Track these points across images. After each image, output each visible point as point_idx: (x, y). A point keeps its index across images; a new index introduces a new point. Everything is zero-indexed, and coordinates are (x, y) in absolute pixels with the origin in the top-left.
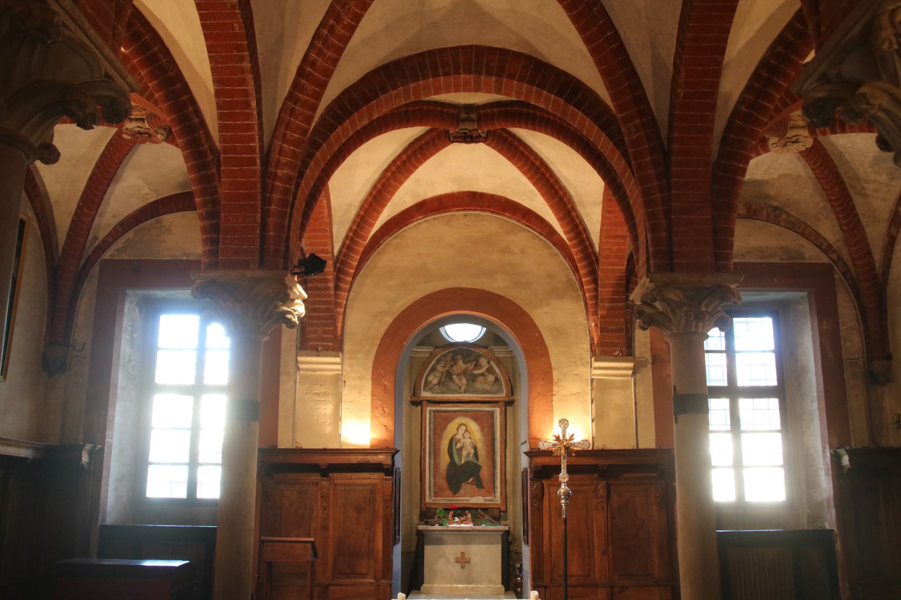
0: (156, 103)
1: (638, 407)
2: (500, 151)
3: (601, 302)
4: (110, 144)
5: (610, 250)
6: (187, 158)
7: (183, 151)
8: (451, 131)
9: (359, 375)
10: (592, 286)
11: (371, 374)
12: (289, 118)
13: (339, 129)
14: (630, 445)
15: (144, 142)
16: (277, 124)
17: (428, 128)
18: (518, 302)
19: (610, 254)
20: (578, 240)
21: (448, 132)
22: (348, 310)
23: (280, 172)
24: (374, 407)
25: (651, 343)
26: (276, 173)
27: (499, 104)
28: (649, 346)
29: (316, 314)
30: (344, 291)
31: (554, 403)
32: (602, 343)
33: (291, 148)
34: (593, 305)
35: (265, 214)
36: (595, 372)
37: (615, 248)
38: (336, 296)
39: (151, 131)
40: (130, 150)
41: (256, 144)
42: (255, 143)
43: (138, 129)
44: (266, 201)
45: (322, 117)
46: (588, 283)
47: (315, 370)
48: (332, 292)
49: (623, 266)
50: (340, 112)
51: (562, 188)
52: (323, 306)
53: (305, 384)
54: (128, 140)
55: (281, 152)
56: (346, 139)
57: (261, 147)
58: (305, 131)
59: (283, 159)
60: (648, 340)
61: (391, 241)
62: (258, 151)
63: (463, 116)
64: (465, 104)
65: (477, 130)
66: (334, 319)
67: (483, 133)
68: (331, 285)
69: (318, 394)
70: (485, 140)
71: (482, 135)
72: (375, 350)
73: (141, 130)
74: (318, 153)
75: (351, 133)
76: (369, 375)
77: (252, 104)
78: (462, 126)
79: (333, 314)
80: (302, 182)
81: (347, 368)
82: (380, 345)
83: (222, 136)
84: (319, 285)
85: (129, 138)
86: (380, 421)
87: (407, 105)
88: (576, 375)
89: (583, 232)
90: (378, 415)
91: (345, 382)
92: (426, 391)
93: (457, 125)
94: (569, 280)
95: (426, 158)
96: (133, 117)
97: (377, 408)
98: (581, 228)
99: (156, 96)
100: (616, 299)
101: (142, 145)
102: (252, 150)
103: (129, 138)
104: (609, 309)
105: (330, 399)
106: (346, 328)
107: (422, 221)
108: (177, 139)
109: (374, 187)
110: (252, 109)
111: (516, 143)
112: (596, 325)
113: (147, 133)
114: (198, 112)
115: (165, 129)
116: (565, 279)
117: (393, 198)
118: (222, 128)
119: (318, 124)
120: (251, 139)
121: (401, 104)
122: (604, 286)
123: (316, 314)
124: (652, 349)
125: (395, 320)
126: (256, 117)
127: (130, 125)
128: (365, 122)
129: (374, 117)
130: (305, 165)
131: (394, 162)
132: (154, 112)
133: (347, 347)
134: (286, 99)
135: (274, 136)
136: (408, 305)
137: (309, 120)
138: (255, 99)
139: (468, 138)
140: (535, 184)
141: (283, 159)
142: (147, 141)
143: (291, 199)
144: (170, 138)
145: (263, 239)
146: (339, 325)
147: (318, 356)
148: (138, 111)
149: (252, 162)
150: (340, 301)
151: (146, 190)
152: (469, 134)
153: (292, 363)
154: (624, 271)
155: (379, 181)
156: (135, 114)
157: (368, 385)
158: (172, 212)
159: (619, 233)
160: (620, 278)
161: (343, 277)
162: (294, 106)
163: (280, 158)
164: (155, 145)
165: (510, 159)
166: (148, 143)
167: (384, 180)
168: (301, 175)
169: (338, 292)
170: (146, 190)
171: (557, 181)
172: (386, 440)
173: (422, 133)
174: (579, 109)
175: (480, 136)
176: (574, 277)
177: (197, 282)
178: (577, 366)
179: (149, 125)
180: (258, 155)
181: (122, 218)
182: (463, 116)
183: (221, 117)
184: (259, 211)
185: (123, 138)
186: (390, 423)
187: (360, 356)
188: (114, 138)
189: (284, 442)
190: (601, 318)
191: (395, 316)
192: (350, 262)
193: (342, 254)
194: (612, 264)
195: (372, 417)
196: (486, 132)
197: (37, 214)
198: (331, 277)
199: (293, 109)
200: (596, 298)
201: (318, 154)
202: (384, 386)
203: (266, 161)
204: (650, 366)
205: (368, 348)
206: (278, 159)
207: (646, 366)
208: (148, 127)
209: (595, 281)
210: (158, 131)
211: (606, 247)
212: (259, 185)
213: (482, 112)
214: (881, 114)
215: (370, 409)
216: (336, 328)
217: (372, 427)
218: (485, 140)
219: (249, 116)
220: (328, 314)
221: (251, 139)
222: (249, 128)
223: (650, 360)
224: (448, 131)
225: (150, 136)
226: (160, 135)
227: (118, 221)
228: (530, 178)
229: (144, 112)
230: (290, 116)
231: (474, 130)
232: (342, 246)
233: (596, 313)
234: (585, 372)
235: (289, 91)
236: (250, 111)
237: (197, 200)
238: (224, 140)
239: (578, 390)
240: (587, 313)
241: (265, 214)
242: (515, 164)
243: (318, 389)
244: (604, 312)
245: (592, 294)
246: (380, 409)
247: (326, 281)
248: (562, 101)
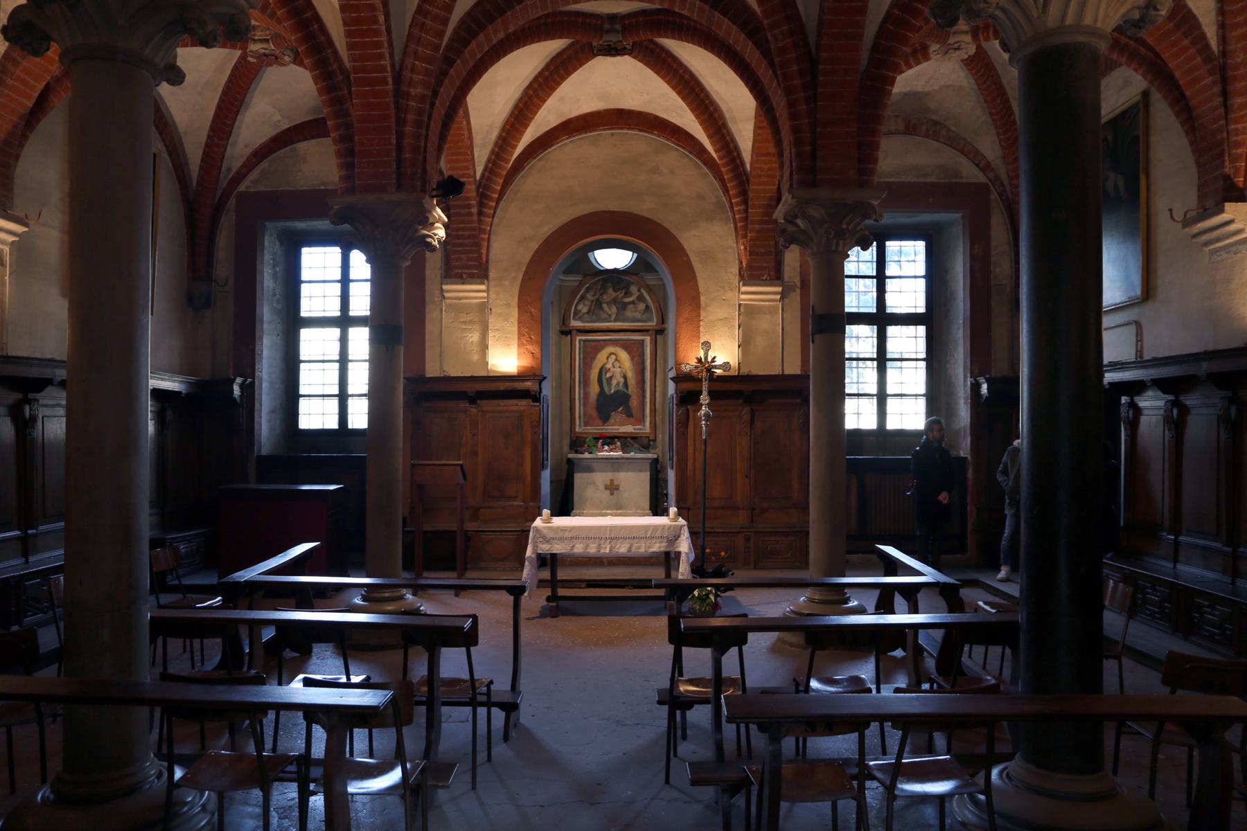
0: (279, 21)
1: (785, 332)
2: (647, 64)
3: (751, 224)
4: (235, 68)
6: (315, 79)
7: (311, 72)
8: (595, 44)
9: (505, 302)
10: (742, 207)
11: (517, 301)
12: (419, 33)
13: (473, 44)
14: (776, 370)
15: (270, 65)
16: (407, 41)
17: (571, 41)
18: (666, 225)
19: (762, 173)
21: (591, 45)
22: (492, 236)
23: (413, 92)
24: (520, 335)
25: (801, 267)
26: (408, 93)
27: (644, 12)
28: (799, 271)
29: (460, 241)
31: (701, 329)
32: (750, 267)
33: (424, 65)
34: (743, 228)
35: (400, 136)
36: (743, 297)
37: (766, 167)
38: (480, 222)
39: (277, 52)
40: (257, 74)
41: (387, 63)
42: (386, 61)
43: (263, 51)
44: (401, 122)
45: (455, 31)
46: (738, 204)
47: (460, 299)
48: (475, 218)
49: (774, 185)
50: (473, 26)
51: (713, 103)
52: (467, 233)
53: (451, 312)
54: (254, 63)
55: (413, 69)
56: (481, 55)
57: (393, 65)
58: (438, 47)
59: (416, 77)
60: (798, 264)
62: (389, 69)
63: (607, 26)
64: (608, 14)
65: (621, 41)
66: (479, 246)
67: (628, 44)
68: (475, 210)
69: (464, 322)
70: (630, 53)
71: (627, 46)
72: (520, 277)
73: (267, 52)
74: (452, 70)
75: (486, 48)
76: (515, 302)
77: (380, 19)
78: (605, 38)
79: (477, 241)
80: (437, 102)
81: (493, 295)
82: (526, 272)
83: (351, 54)
84: (463, 211)
85: (255, 60)
86: (527, 349)
87: (546, 16)
88: (724, 300)
89: (733, 149)
90: (525, 342)
91: (491, 309)
92: (576, 320)
93: (601, 37)
95: (569, 73)
96: (256, 38)
97: (524, 335)
98: (732, 145)
99: (279, 13)
101: (269, 68)
102: (383, 69)
103: (255, 60)
105: (476, 327)
106: (491, 254)
107: (568, 141)
108: (304, 59)
109: (516, 106)
110: (381, 25)
111: (664, 55)
112: (745, 248)
113: (273, 55)
114: (323, 29)
115: (291, 50)
117: (536, 117)
118: (351, 47)
119: (451, 40)
120: (381, 57)
121: (538, 15)
123: (460, 241)
124: (801, 273)
125: (539, 246)
126: (385, 33)
127: (254, 47)
128: (501, 35)
129: (510, 30)
130: (439, 83)
131: (536, 79)
132: (278, 32)
133: (492, 274)
134: (415, 13)
135: (405, 53)
136: (554, 230)
137: (441, 35)
138: (382, 13)
139: (613, 51)
140: (684, 99)
141: (416, 77)
142: (274, 63)
143: (426, 119)
144: (297, 61)
145: (400, 162)
146: (484, 251)
147: (463, 284)
148: (262, 31)
149: (383, 81)
150: (483, 227)
151: (278, 117)
152: (613, 46)
153: (437, 292)
155: (521, 99)
156: (259, 35)
157: (515, 312)
158: (306, 139)
161: (486, 202)
162: (424, 20)
163: (413, 76)
164: (283, 68)
165: (658, 72)
166: (275, 66)
167: (526, 98)
168: (435, 94)
169: (482, 218)
170: (278, 117)
171: (708, 96)
172: (533, 367)
173: (564, 47)
174: (725, 16)
175: (625, 48)
176: (724, 198)
177: (335, 207)
178: (725, 291)
179: (274, 46)
180: (390, 74)
181: (255, 147)
182: (607, 26)
183: (349, 34)
184: (394, 132)
185: (249, 61)
186: (536, 349)
187: (506, 283)
188: (238, 62)
189: (432, 370)
190: (751, 240)
191: (541, 242)
192: (493, 186)
193: (485, 178)
195: (519, 345)
196: (631, 44)
197: (166, 146)
198: (474, 202)
199: (423, 24)
200: (745, 219)
201: (452, 71)
202: (531, 313)
203: (398, 81)
204: (798, 291)
205: (513, 274)
206: (411, 78)
207: (795, 291)
208: (274, 48)
210: (285, 53)
212: (392, 106)
213: (627, 22)
214: (998, 13)
215: (516, 337)
216: (480, 254)
217: (519, 354)
218: (630, 52)
219: (377, 33)
220: (473, 241)
221: (381, 57)
222: (378, 45)
223: (799, 284)
224: (591, 44)
225: (276, 58)
226: (287, 57)
227: (251, 150)
228: (679, 93)
229: (268, 32)
230: (421, 32)
231: (619, 41)
233: (745, 236)
234: (732, 296)
235: (418, 4)
236: (379, 27)
237: (330, 123)
238: (353, 59)
239: (726, 316)
240: (736, 236)
241: (400, 136)
242: (663, 77)
243: (464, 317)
244: (754, 235)
246: (527, 336)
247: (470, 206)
248: (707, 7)
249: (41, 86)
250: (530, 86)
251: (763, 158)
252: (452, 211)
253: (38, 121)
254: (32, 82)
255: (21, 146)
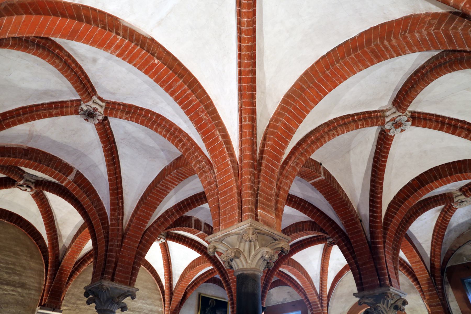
5: (416, 268)
10: (418, 286)
19: (418, 270)
20: (402, 267)
30: (325, 307)
37: (418, 267)
38: (322, 310)
48: (320, 308)
49: (426, 274)
61: (339, 283)
68: (319, 306)
78: (328, 241)
84: (316, 306)
93: (326, 241)
94: (410, 285)
98: (402, 262)
100: (431, 290)
104: (430, 295)
116: (408, 284)
122: (423, 285)
136: (350, 308)
154: (428, 276)
159: (417, 261)
160: (428, 280)
169: (323, 308)
194: (421, 274)
198: (318, 303)
200: (421, 291)
209: (418, 283)
211: (415, 268)
232: (320, 290)
245: (419, 289)
247: (317, 305)
249: (183, 293)
250: (322, 260)
251: (415, 264)
252: (312, 307)
253: (184, 302)
254: (180, 293)
255: (179, 310)
